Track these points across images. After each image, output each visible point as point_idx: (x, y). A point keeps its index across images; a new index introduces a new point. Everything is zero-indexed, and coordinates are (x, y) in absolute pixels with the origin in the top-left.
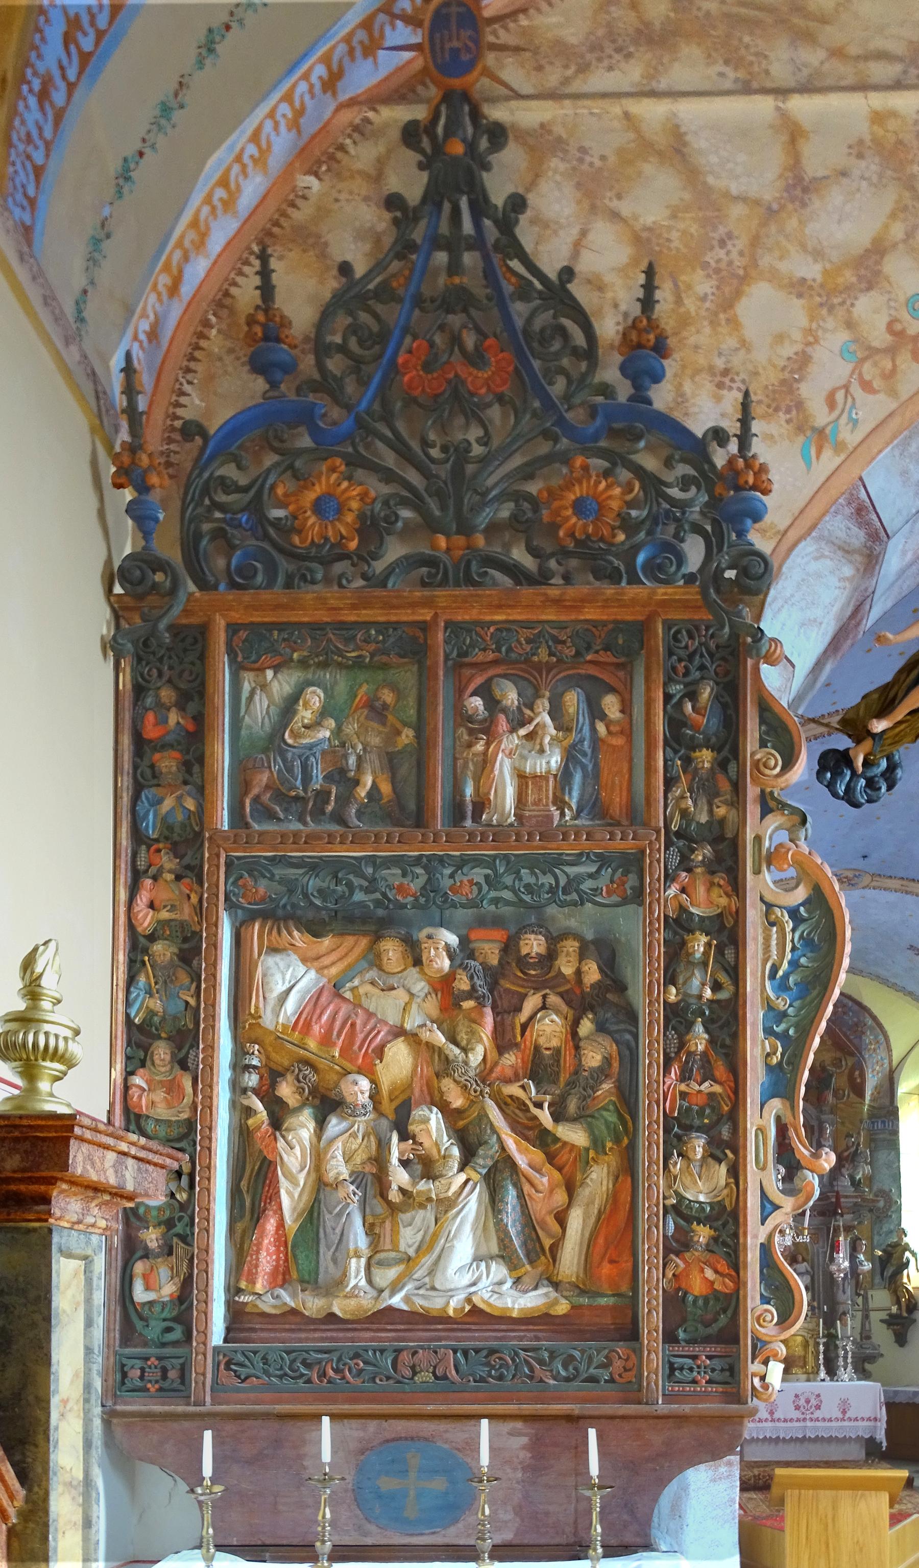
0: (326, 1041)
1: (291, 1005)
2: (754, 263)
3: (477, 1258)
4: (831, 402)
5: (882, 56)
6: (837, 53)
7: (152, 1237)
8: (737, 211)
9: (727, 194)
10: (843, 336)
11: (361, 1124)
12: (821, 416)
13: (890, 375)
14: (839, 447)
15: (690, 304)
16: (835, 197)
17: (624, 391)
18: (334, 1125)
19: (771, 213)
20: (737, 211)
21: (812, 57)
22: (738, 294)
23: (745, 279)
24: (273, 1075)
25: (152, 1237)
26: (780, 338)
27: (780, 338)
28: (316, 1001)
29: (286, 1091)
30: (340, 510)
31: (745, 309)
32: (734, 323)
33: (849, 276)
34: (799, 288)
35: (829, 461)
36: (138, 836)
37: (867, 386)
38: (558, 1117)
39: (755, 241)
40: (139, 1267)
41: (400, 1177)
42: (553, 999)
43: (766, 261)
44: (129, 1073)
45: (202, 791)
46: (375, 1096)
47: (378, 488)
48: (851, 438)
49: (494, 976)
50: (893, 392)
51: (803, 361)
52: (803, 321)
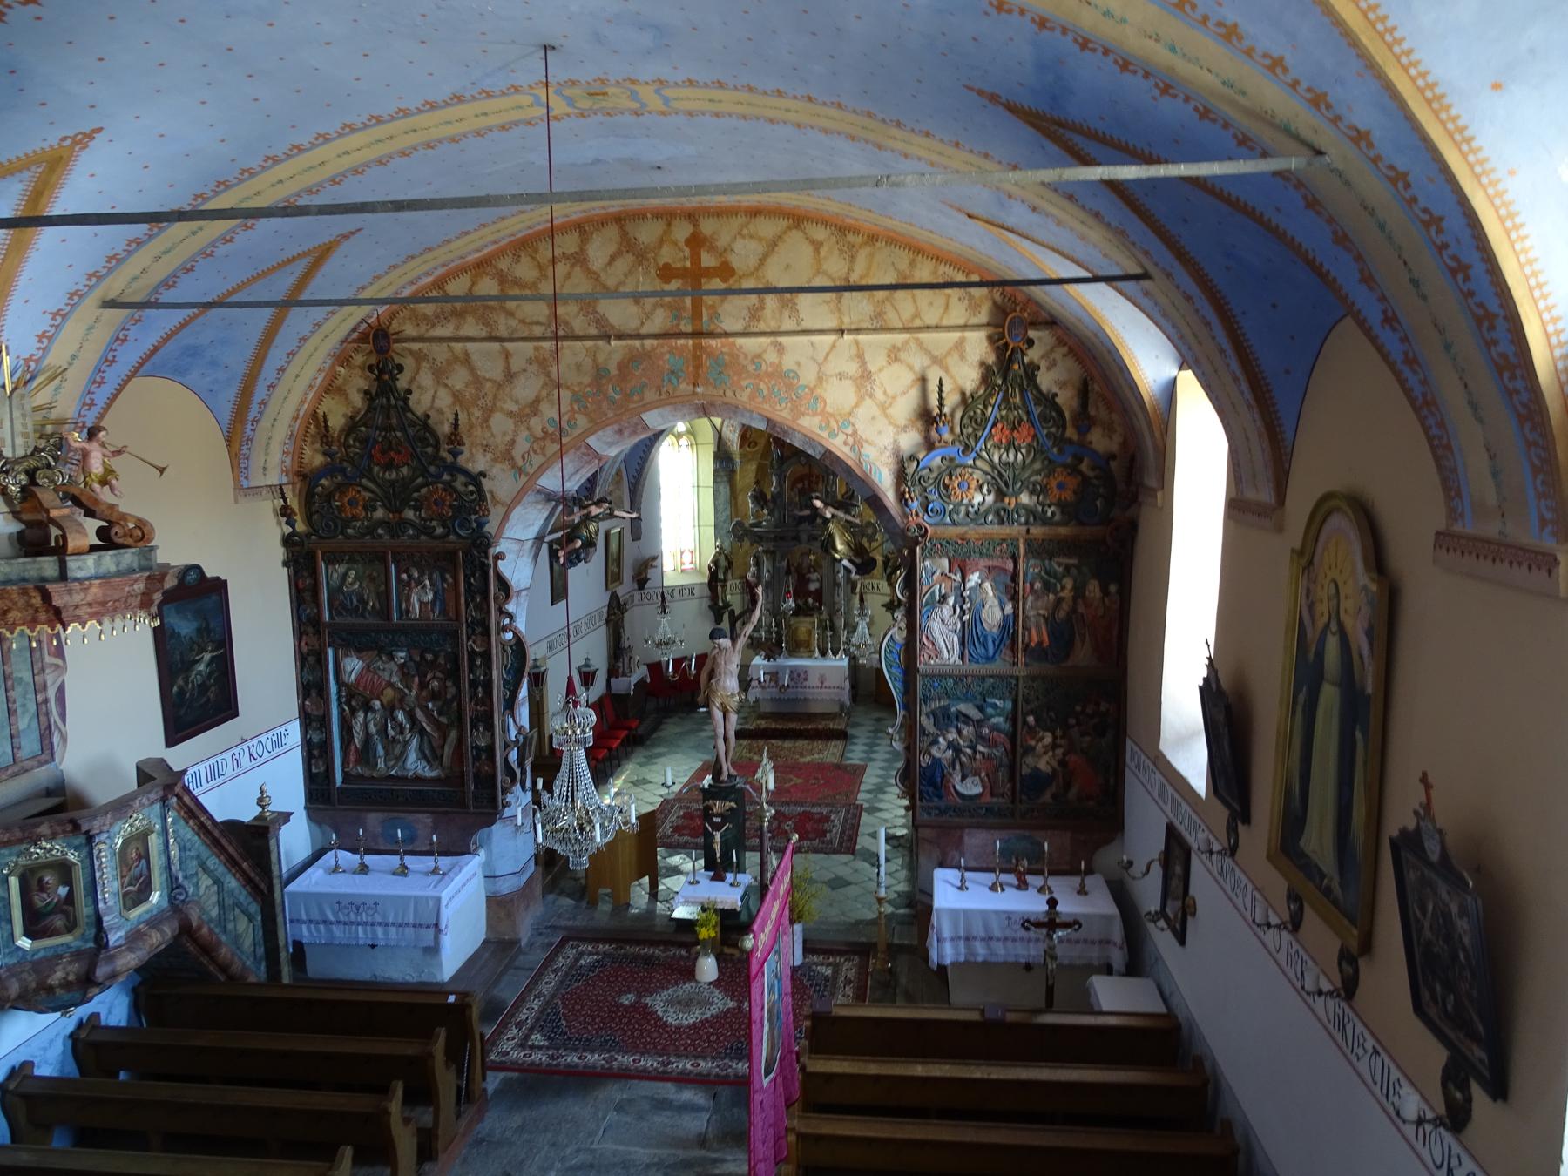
0: (365, 687)
1: (353, 677)
2: (495, 404)
3: (418, 759)
4: (523, 457)
5: (538, 323)
6: (523, 321)
7: (316, 752)
8: (489, 385)
9: (484, 378)
10: (527, 433)
11: (378, 716)
12: (520, 463)
13: (543, 448)
14: (527, 474)
15: (473, 419)
16: (522, 379)
17: (449, 458)
18: (370, 716)
19: (499, 386)
20: (489, 385)
21: (513, 323)
22: (489, 417)
23: (492, 411)
24: (351, 696)
25: (316, 752)
26: (504, 434)
27: (504, 434)
28: (361, 674)
29: (353, 703)
30: (357, 503)
31: (492, 422)
32: (489, 427)
33: (527, 410)
34: (511, 414)
35: (524, 479)
36: (299, 619)
37: (535, 452)
38: (440, 714)
39: (495, 397)
40: (313, 761)
41: (391, 733)
42: (438, 674)
43: (499, 404)
44: (304, 700)
45: (318, 605)
46: (382, 705)
47: (367, 495)
48: (531, 471)
49: (418, 665)
50: (544, 455)
51: (513, 442)
52: (512, 427)
